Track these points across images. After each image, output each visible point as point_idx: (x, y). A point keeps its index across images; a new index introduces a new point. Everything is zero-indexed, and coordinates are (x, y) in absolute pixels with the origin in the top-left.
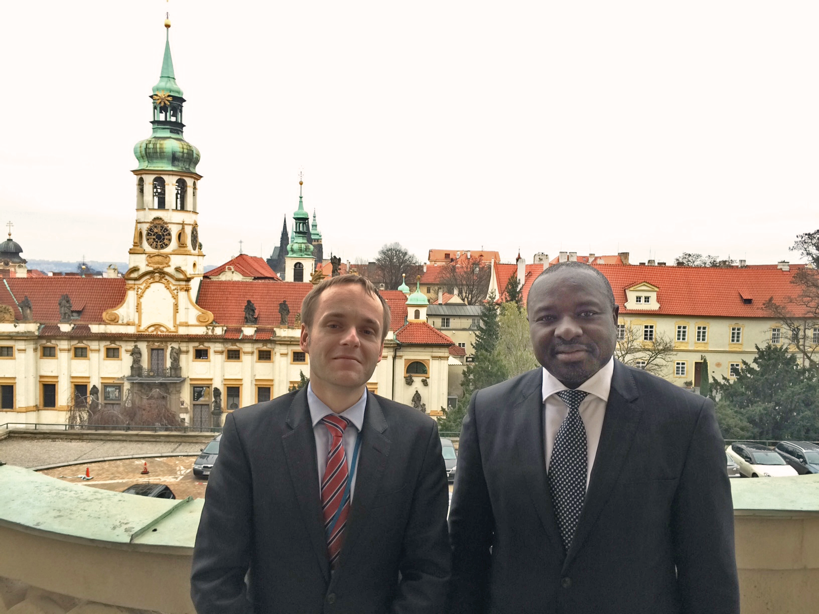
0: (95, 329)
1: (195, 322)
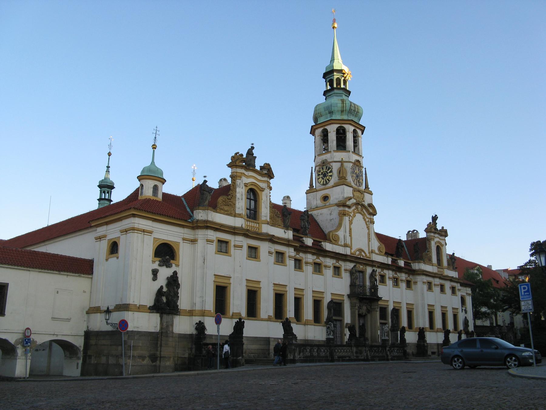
1: (377, 251)
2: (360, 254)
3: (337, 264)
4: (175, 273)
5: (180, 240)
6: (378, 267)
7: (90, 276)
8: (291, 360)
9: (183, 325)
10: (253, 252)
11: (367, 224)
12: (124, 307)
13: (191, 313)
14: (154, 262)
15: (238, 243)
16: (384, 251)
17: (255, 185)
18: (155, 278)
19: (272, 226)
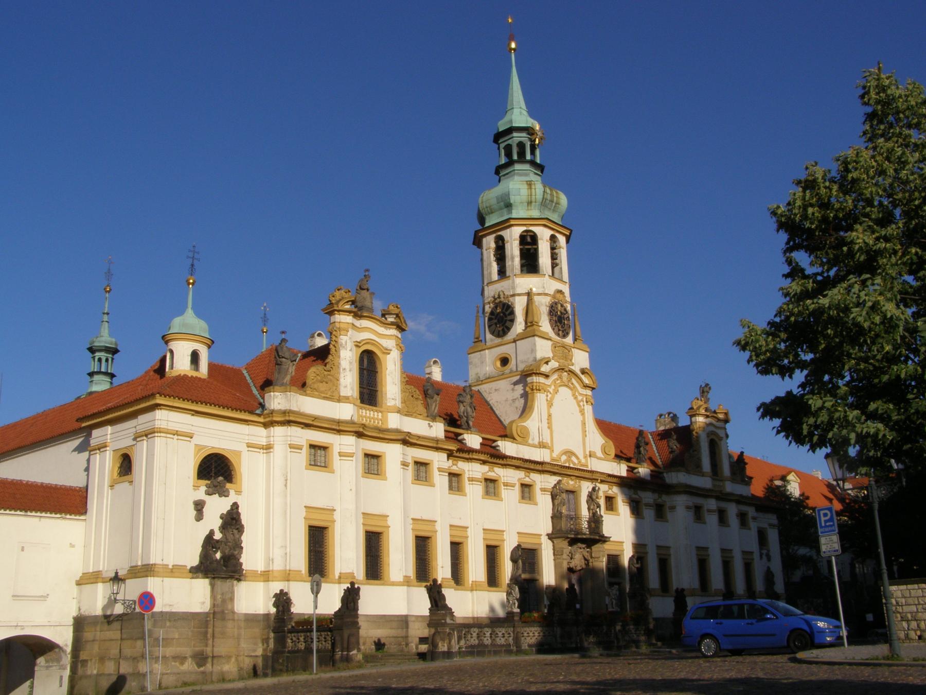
1: (599, 454)
2: (569, 460)
4: (235, 506)
5: (243, 448)
6: (602, 482)
7: (82, 517)
8: (444, 652)
9: (252, 599)
10: (373, 463)
11: (579, 406)
12: (147, 570)
13: (266, 576)
14: (196, 487)
15: (346, 450)
16: (613, 453)
17: (373, 344)
18: (199, 516)
19: (406, 415)
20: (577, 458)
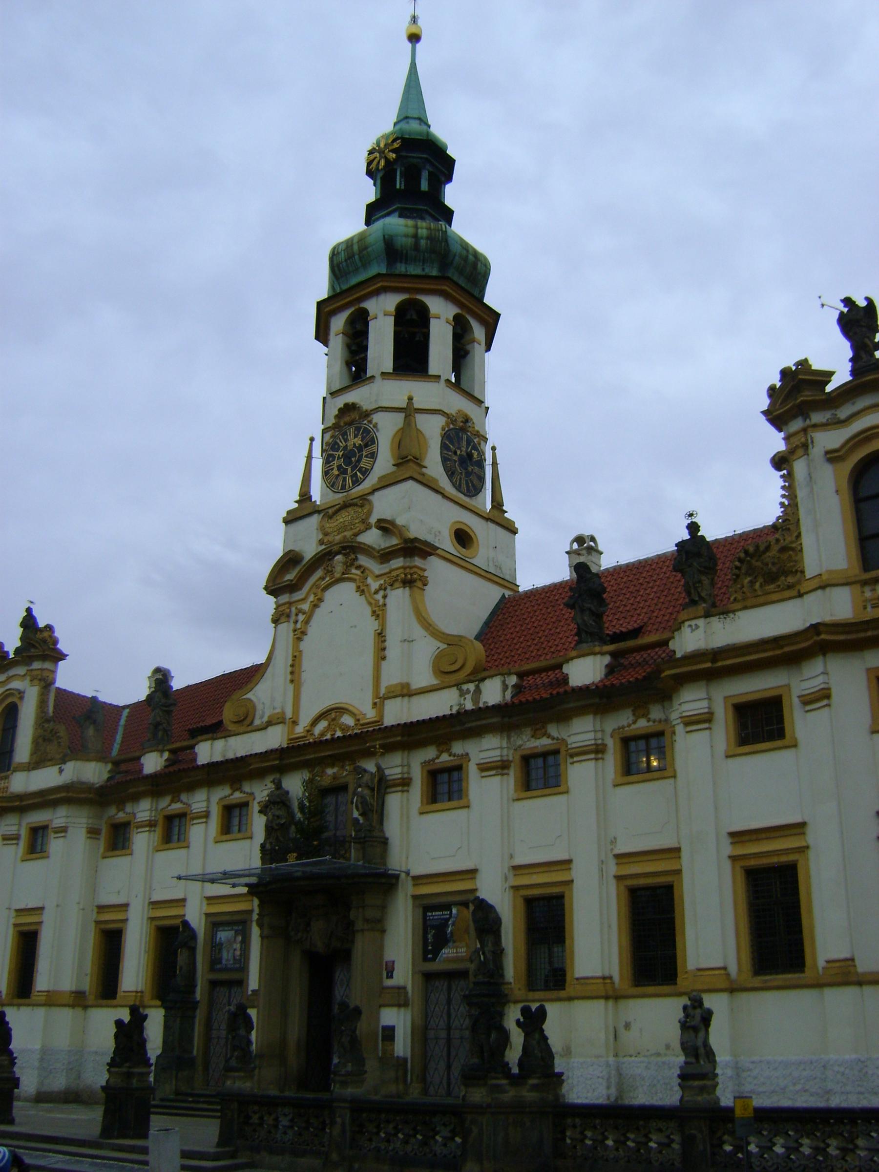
0: (208, 752)
3: (237, 795)
11: (370, 604)
20: (352, 714)
